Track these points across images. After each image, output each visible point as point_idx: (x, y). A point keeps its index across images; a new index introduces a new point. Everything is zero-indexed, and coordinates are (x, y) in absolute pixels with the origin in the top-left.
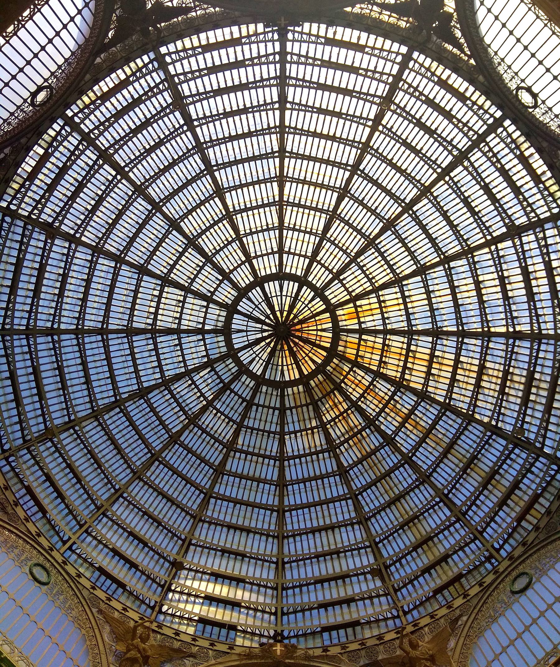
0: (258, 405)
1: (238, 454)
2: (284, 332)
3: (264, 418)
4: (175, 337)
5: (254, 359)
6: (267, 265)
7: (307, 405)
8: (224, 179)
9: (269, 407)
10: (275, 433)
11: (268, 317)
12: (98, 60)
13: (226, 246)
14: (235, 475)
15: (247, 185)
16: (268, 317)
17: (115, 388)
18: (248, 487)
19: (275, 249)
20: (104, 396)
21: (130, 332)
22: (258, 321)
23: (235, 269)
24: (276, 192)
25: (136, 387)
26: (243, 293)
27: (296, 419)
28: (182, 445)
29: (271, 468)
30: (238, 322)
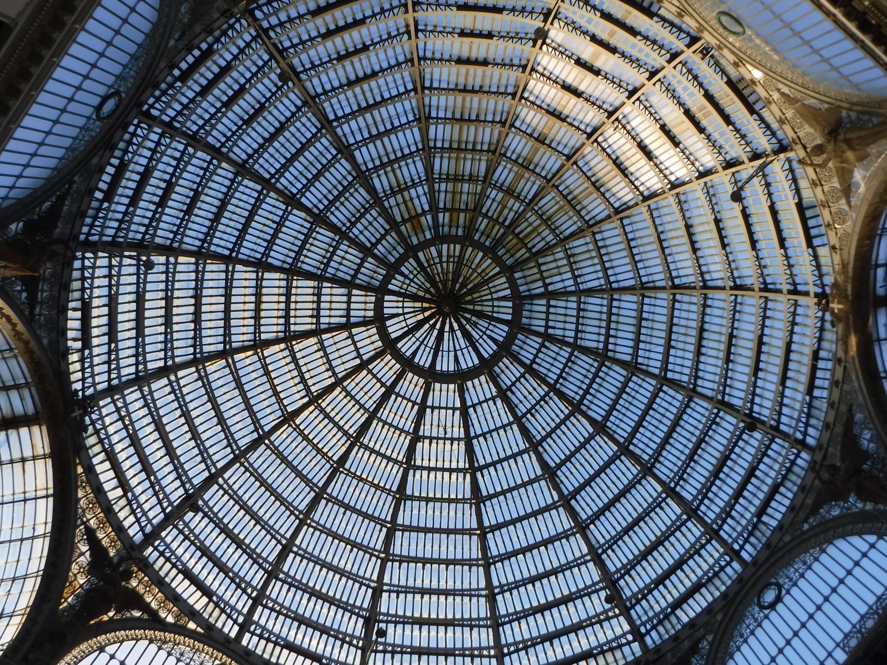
0: (547, 327)
1: (611, 347)
2: (449, 301)
3: (562, 318)
4: (475, 442)
5: (489, 337)
6: (368, 341)
7: (539, 265)
8: (272, 417)
9: (548, 313)
10: (579, 303)
11: (433, 327)
12: (170, 619)
13: (353, 398)
14: (636, 348)
15: (273, 387)
16: (433, 327)
17: (547, 509)
18: (649, 332)
19: (345, 334)
20: (560, 521)
21: (478, 498)
22: (440, 339)
23: (379, 380)
24: (276, 348)
25: (543, 483)
26: (408, 364)
27: (558, 278)
28: (606, 418)
29: (623, 305)
30: (445, 364)
